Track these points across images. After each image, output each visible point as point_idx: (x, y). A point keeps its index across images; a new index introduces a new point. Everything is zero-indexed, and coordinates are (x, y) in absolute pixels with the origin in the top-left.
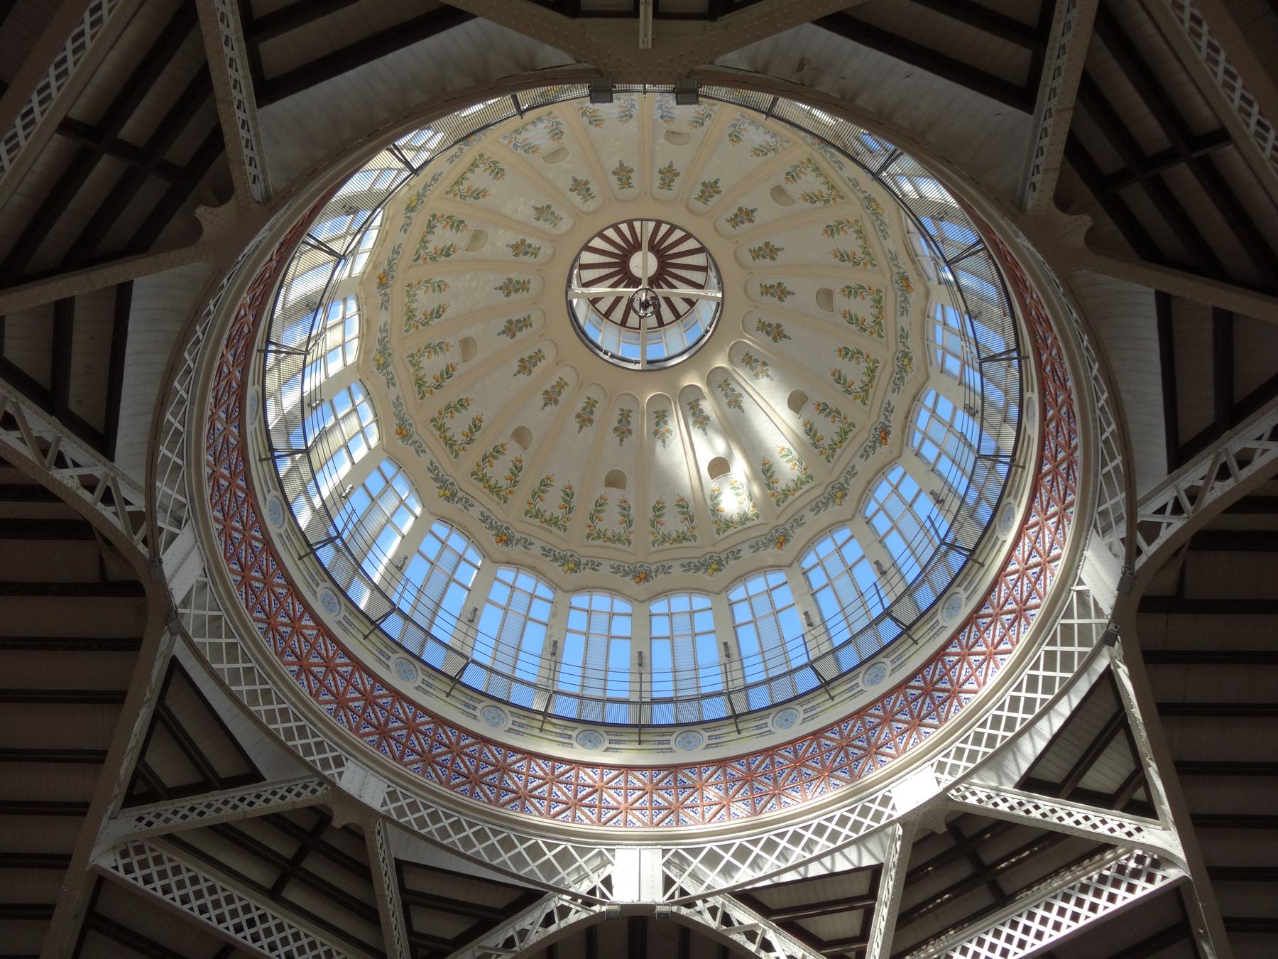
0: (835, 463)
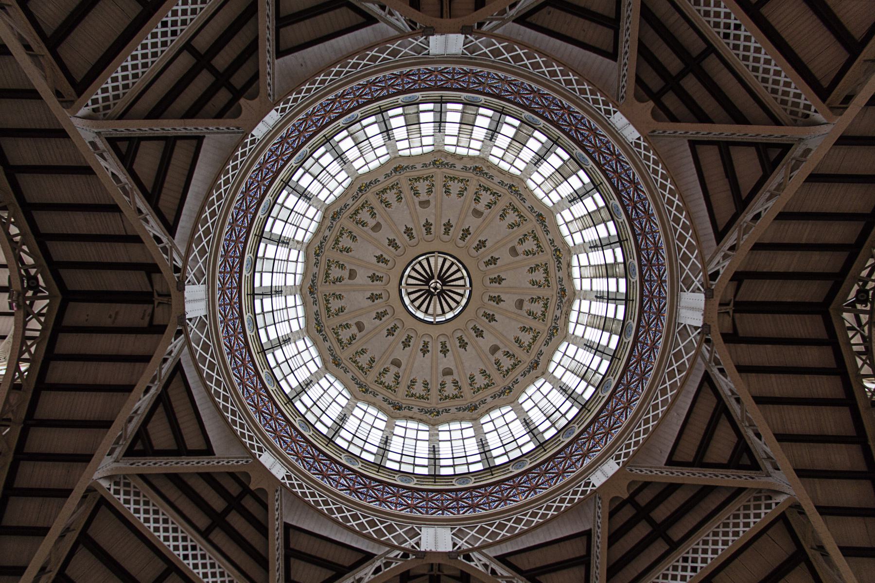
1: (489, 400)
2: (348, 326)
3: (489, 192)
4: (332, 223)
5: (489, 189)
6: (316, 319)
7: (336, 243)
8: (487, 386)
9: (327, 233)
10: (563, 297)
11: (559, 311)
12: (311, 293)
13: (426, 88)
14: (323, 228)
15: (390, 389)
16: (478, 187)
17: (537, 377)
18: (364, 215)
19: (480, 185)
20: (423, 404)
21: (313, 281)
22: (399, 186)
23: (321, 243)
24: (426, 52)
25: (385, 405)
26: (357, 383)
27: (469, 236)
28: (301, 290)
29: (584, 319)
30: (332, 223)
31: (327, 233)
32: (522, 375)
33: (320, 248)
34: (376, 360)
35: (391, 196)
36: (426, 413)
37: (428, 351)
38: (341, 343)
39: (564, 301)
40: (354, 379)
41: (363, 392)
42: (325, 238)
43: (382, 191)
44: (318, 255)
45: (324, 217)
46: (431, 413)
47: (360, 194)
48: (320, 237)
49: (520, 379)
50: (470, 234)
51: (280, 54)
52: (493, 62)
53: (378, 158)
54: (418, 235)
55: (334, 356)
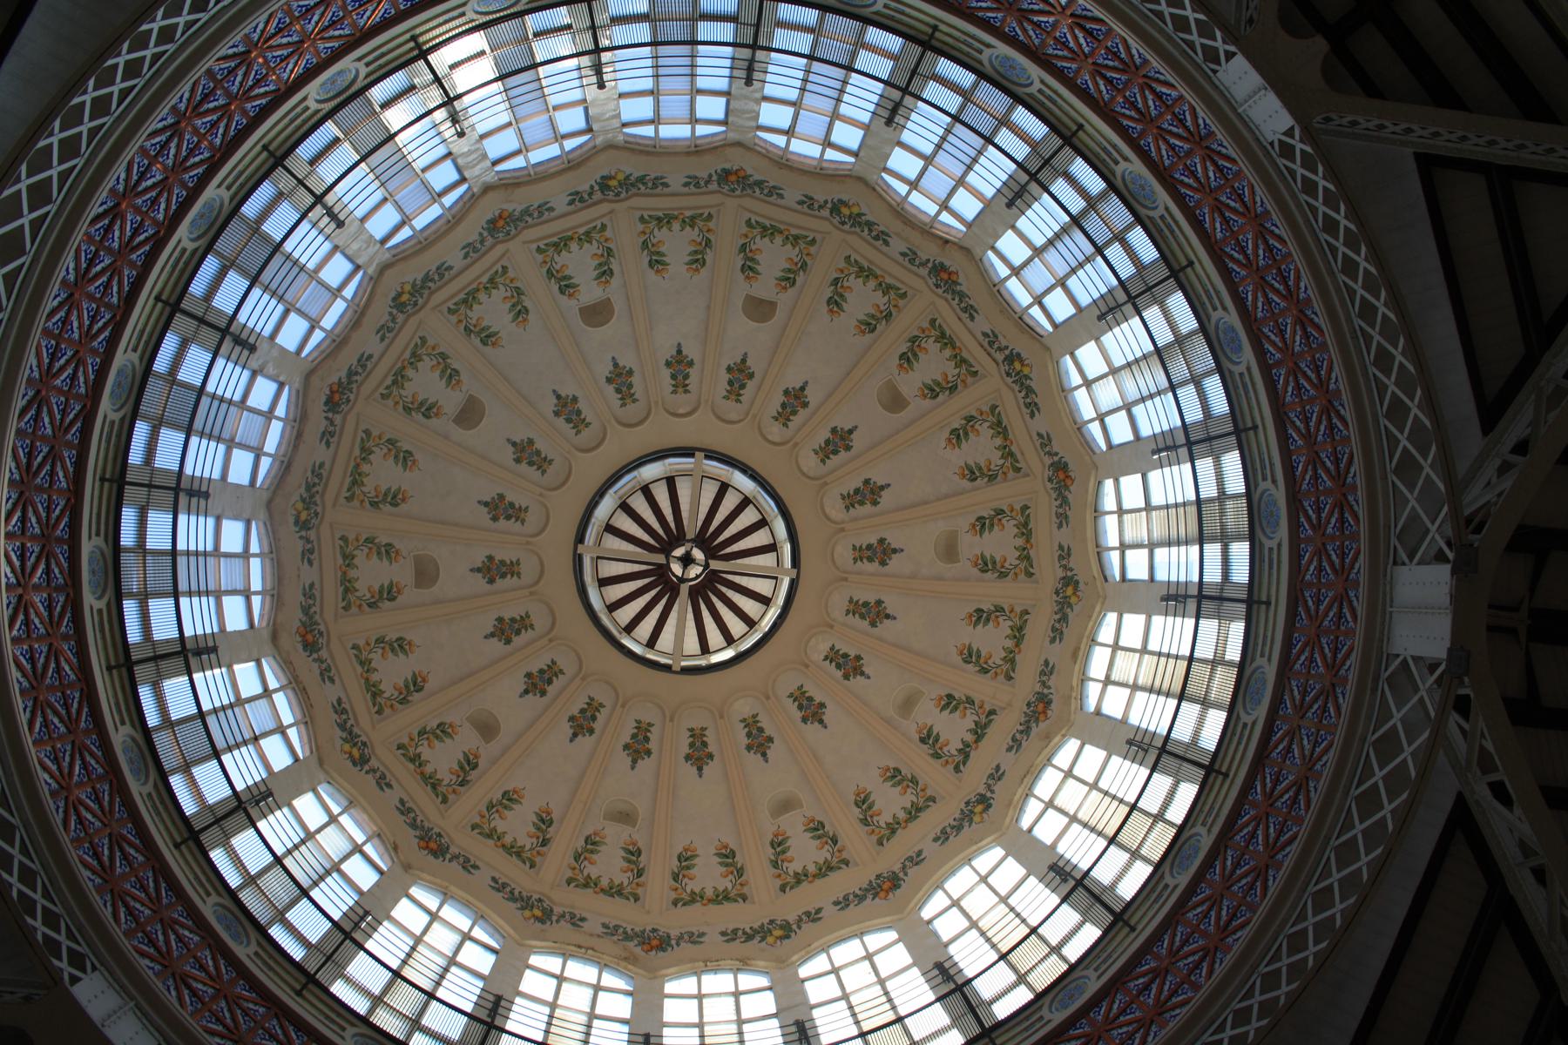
2: (605, 273)
3: (970, 738)
4: (923, 264)
7: (861, 269)
8: (374, 691)
9: (897, 246)
12: (725, 175)
13: (1300, 557)
14: (916, 238)
15: (395, 382)
17: (396, 848)
18: (934, 364)
19: (992, 712)
21: (759, 183)
23: (870, 224)
24: (1403, 555)
25: (348, 358)
27: (839, 674)
28: (739, 144)
30: (923, 264)
31: (897, 246)
32: (402, 802)
34: (488, 350)
35: (982, 448)
36: (308, 488)
37: (495, 519)
39: (631, 944)
41: (399, 295)
43: (999, 423)
44: (835, 209)
45: (947, 242)
46: (308, 502)
47: (1000, 357)
48: (885, 222)
49: (392, 797)
50: (846, 677)
51: (1428, 164)
52: (1363, 740)
53: (1101, 418)
54: (855, 519)
55: (519, 219)
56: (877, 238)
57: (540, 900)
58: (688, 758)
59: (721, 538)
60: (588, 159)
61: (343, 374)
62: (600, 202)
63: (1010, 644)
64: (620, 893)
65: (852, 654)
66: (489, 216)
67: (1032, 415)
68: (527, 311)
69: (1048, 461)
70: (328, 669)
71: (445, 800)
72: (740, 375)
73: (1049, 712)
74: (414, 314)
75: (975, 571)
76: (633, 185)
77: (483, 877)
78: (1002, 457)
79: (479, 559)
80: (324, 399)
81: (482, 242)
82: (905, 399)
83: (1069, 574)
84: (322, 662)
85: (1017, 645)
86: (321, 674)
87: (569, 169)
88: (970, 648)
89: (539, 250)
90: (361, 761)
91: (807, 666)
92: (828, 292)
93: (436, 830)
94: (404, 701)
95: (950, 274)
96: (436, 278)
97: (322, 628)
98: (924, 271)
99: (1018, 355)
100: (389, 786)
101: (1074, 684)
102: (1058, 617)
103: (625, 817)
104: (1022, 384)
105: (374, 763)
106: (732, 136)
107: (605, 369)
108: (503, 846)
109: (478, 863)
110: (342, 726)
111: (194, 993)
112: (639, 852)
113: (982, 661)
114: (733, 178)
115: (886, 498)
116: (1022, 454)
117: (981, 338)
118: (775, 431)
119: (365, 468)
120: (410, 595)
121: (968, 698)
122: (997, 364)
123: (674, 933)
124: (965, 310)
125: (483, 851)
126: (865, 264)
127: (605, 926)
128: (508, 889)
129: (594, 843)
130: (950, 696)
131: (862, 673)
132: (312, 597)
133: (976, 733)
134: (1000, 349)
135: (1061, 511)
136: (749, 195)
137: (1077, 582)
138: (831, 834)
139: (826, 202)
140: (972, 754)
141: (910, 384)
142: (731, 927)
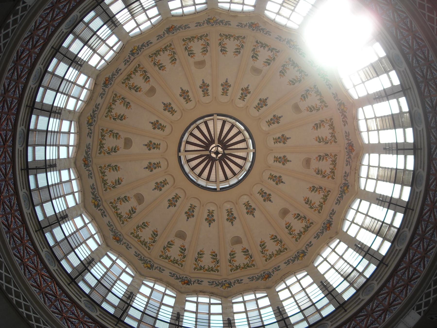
0: (130, 237)
1: (283, 266)
4: (104, 90)
5: (266, 45)
6: (93, 194)
7: (109, 111)
8: (280, 252)
9: (99, 101)
10: (351, 152)
11: (349, 167)
12: (86, 165)
15: (176, 263)
16: (255, 44)
17: (331, 238)
19: (257, 42)
20: (213, 276)
21: (86, 153)
22: (172, 47)
23: (94, 111)
25: (172, 280)
26: (141, 259)
27: (248, 95)
28: (75, 163)
29: (374, 173)
30: (104, 90)
31: (99, 101)
32: (315, 238)
33: (93, 117)
34: (159, 233)
36: (218, 285)
38: (120, 218)
40: (137, 255)
41: (148, 268)
42: (97, 106)
43: (155, 54)
45: (95, 84)
47: (132, 58)
49: (314, 241)
50: (249, 93)
56: (98, 108)
57: (341, 188)
58: (284, 143)
59: (205, 141)
60: (90, 214)
61: (178, 281)
62: (103, 206)
63: (232, 39)
64: (335, 161)
65: (241, 92)
66: (116, 243)
67: (151, 43)
68: (144, 223)
69: (166, 35)
70: (275, 268)
71: (312, 223)
72: (151, 146)
73: (256, 23)
74: (153, 261)
75: (208, 54)
76: (95, 196)
77: (336, 208)
78: (167, 51)
79: (228, 224)
80: (188, 286)
81: (125, 243)
82: (151, 87)
83: (206, 22)
84: (274, 271)
85: (232, 36)
86: (277, 270)
87: (95, 219)
88: (235, 52)
89: (123, 223)
90: (304, 253)
91: (247, 106)
92: (118, 121)
93: (323, 225)
94: (281, 241)
95: (106, 80)
96: (140, 256)
97: (262, 273)
98: (107, 90)
99: (131, 51)
100: (310, 242)
101: (245, 15)
102: (221, 24)
103: (308, 162)
104: (141, 48)
105: (304, 249)
106: (73, 165)
107: (157, 192)
108: (324, 202)
109: (332, 210)
110: (294, 261)
111: (394, 300)
112: (319, 156)
113: (239, 48)
114: (86, 162)
115: (185, 88)
116: (165, 44)
117: (127, 65)
118: (168, 130)
119: (206, 267)
120: (245, 245)
121: (252, 51)
122: (135, 58)
123: (346, 142)
124: (118, 73)
125: (327, 209)
126: (107, 110)
127: (347, 165)
128: (339, 199)
129: (319, 171)
130: (252, 57)
131: (248, 87)
132: (253, 278)
133: (265, 47)
134: (130, 58)
135: (184, 28)
136: (91, 156)
137: (208, 19)
138: (305, 92)
139: (89, 128)
140: (272, 47)
141: (145, 87)
142: (342, 123)
